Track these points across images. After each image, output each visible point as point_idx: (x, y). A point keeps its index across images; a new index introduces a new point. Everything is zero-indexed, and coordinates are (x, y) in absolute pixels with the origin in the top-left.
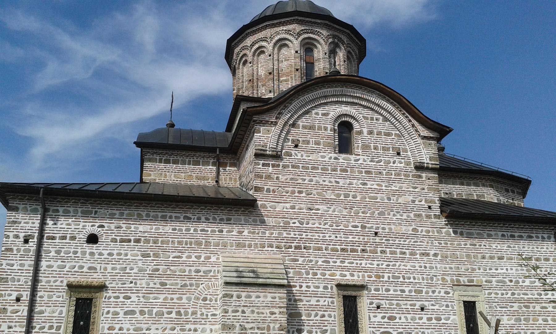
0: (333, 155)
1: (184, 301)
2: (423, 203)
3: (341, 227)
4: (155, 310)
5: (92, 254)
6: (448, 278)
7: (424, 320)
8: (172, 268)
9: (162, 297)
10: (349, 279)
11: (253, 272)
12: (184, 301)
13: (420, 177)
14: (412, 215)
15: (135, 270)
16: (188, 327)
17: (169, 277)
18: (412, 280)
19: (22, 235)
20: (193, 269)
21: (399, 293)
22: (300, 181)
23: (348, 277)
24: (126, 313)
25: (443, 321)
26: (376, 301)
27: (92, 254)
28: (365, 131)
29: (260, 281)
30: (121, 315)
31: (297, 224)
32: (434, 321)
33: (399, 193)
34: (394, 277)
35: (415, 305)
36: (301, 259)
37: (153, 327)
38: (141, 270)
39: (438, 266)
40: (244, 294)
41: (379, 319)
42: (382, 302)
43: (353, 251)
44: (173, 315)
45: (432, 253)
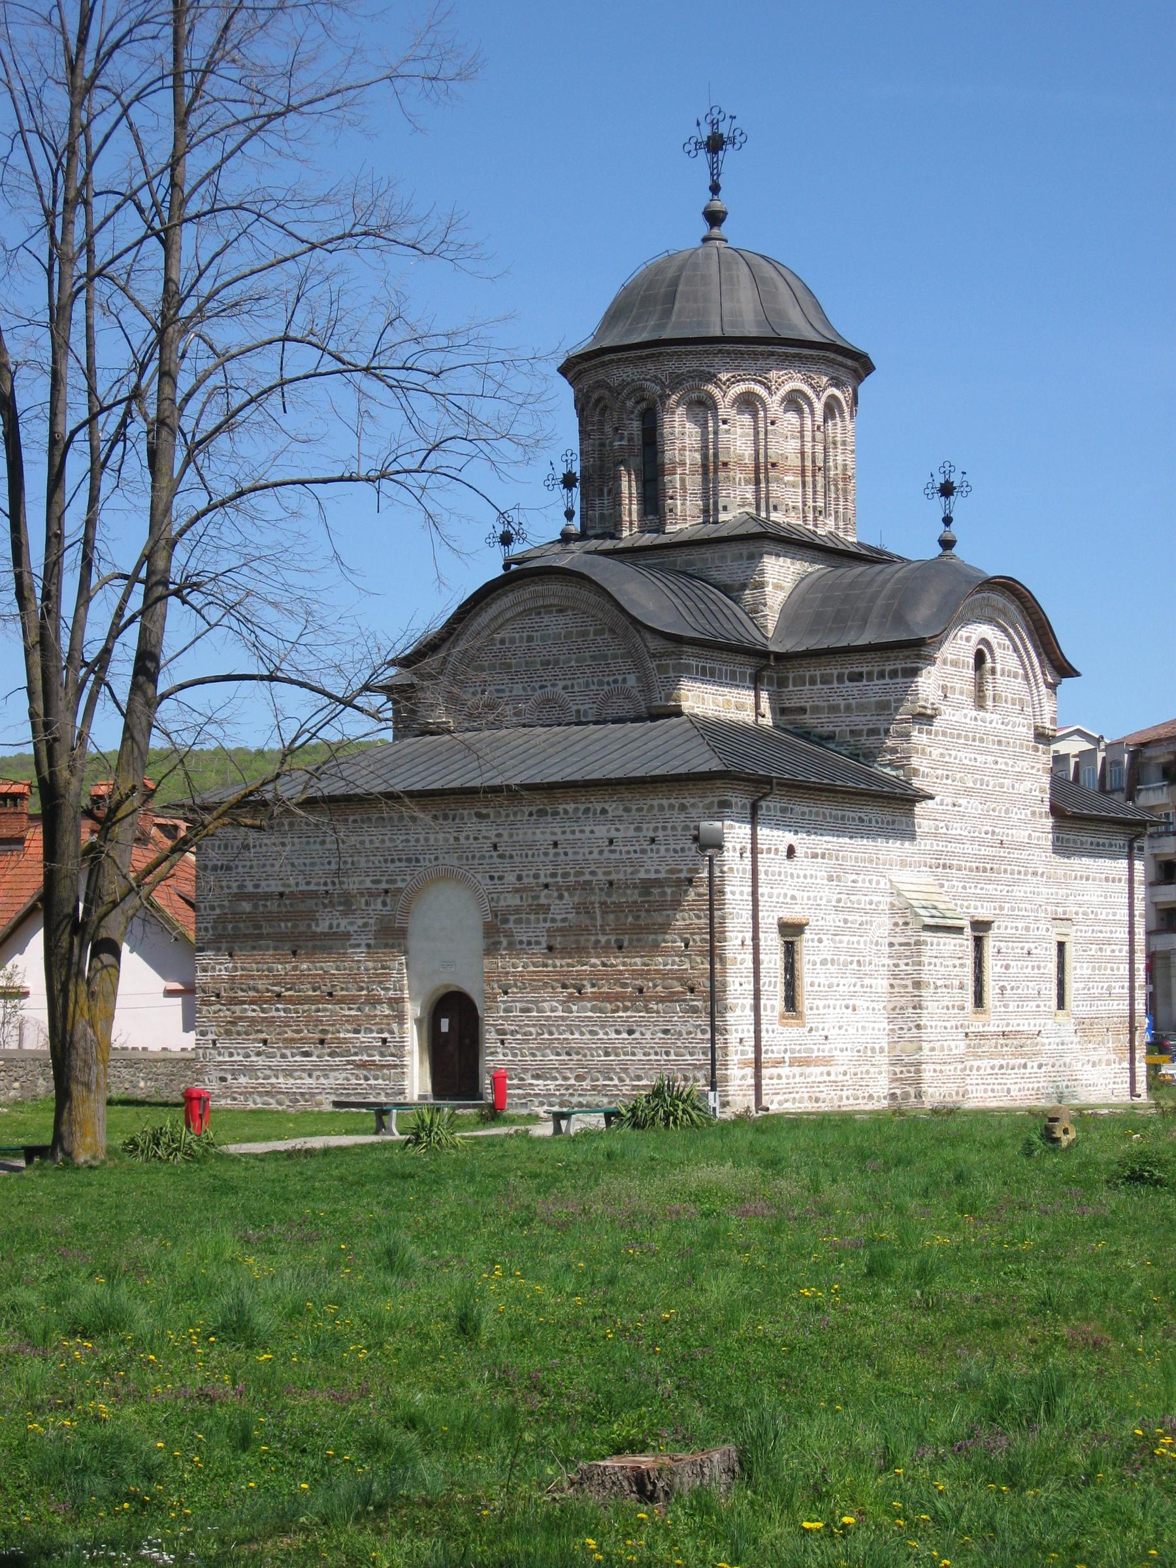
0: (974, 713)
1: (862, 946)
2: (1037, 793)
3: (977, 834)
4: (842, 958)
5: (792, 875)
6: (1049, 908)
7: (1029, 970)
8: (852, 898)
9: (845, 939)
10: (983, 914)
11: (935, 908)
12: (862, 946)
13: (1037, 750)
14: (1029, 812)
15: (824, 902)
16: (867, 981)
17: (851, 910)
18: (1023, 913)
19: (738, 846)
20: (868, 898)
21: (1014, 931)
22: (947, 759)
23: (980, 910)
24: (822, 964)
25: (1042, 971)
26: (997, 944)
27: (792, 875)
28: (998, 667)
29: (950, 922)
30: (818, 966)
31: (944, 830)
32: (1036, 971)
33: (1020, 777)
34: (1013, 909)
35: (1022, 948)
36: (946, 884)
37: (842, 981)
38: (829, 901)
39: (1044, 890)
40: (935, 940)
41: (997, 969)
42: (1002, 944)
43: (985, 870)
44: (855, 966)
45: (1040, 871)
